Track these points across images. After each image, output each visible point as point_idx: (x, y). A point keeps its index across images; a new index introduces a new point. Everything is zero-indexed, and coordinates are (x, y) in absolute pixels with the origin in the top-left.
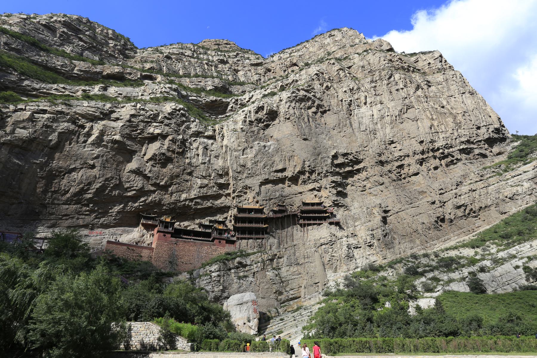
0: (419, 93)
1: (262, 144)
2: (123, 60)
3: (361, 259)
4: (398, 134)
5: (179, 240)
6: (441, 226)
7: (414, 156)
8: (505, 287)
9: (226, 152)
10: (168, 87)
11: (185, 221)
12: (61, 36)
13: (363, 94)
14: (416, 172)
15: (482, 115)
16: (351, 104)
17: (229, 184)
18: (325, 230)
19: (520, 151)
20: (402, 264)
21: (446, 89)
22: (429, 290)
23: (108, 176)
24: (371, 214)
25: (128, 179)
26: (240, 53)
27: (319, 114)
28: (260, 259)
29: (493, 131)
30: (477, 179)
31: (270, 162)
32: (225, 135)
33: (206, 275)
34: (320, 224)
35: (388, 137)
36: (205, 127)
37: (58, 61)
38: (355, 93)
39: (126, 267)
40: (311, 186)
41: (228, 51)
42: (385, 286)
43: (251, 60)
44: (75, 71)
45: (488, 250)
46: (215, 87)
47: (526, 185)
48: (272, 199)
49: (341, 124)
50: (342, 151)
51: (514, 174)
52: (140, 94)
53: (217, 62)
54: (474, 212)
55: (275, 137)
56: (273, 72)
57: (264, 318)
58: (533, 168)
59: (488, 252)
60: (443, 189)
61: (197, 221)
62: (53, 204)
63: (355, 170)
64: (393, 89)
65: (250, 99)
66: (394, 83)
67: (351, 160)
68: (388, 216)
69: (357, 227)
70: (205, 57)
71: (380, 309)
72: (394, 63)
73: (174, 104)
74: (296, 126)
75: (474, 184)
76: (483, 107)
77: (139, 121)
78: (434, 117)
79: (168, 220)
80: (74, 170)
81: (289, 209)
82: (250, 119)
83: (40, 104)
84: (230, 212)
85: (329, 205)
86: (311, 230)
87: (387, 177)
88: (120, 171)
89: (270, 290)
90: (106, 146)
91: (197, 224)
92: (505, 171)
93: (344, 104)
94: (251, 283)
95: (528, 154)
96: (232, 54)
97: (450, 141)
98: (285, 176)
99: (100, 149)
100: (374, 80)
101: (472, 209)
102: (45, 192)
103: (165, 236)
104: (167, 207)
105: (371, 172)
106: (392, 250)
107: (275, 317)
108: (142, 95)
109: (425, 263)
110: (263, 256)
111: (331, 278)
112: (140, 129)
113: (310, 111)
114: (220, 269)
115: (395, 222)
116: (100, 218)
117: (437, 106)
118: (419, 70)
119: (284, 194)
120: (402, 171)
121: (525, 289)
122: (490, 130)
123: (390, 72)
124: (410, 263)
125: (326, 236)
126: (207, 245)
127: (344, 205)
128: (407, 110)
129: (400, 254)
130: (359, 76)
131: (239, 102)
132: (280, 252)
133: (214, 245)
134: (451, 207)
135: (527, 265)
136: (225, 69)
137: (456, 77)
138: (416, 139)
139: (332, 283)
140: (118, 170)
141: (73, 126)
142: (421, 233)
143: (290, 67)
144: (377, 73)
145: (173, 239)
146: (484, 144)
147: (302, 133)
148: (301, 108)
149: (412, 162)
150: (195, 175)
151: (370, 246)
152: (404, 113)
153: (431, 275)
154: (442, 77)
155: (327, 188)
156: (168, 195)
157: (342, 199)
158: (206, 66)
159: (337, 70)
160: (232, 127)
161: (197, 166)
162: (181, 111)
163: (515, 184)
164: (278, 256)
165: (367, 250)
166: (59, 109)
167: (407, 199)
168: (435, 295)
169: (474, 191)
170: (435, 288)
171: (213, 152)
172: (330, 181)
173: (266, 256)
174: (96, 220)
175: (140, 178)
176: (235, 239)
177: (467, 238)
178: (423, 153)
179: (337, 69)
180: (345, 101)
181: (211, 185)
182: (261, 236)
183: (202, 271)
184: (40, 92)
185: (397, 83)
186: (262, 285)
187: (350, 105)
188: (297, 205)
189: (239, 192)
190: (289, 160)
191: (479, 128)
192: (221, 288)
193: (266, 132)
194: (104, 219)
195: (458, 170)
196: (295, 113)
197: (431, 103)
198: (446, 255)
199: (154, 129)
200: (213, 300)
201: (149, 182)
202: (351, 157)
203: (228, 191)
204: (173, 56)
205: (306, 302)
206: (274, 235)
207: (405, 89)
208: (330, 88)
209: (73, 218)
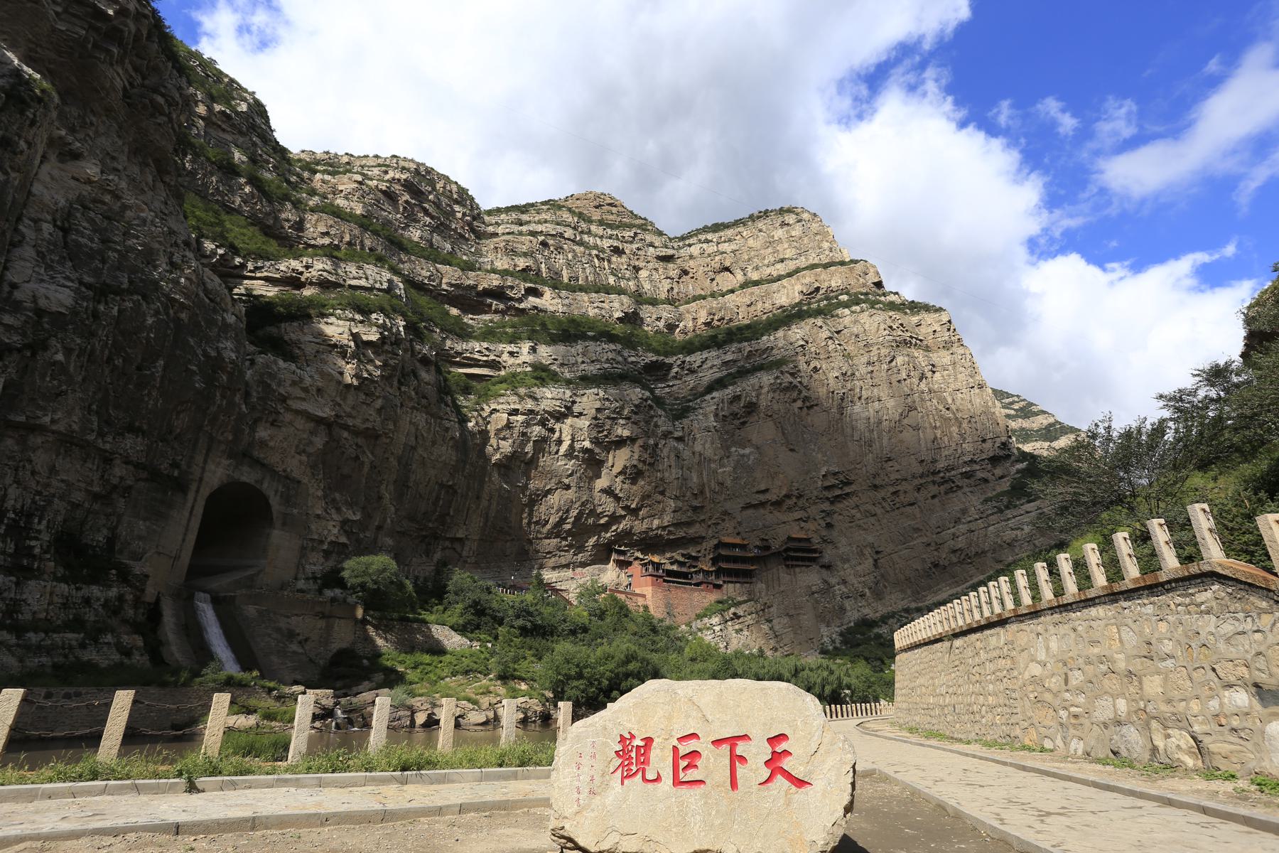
1: (742, 452)
12: (405, 208)
20: (895, 620)
24: (861, 554)
33: (708, 629)
40: (797, 515)
44: (444, 286)
47: (1027, 529)
52: (580, 360)
53: (608, 251)
61: (668, 555)
62: (537, 538)
64: (894, 380)
65: (703, 362)
66: (895, 370)
78: (938, 424)
80: (549, 492)
84: (704, 544)
92: (1007, 507)
99: (573, 461)
117: (941, 407)
118: (921, 340)
122: (997, 445)
126: (696, 590)
130: (850, 348)
133: (702, 590)
140: (591, 489)
158: (596, 260)
162: (649, 402)
167: (901, 538)
175: (611, 499)
178: (921, 477)
182: (749, 580)
184: (464, 358)
187: (842, 399)
191: (984, 441)
202: (842, 477)
204: (551, 242)
209: (555, 555)
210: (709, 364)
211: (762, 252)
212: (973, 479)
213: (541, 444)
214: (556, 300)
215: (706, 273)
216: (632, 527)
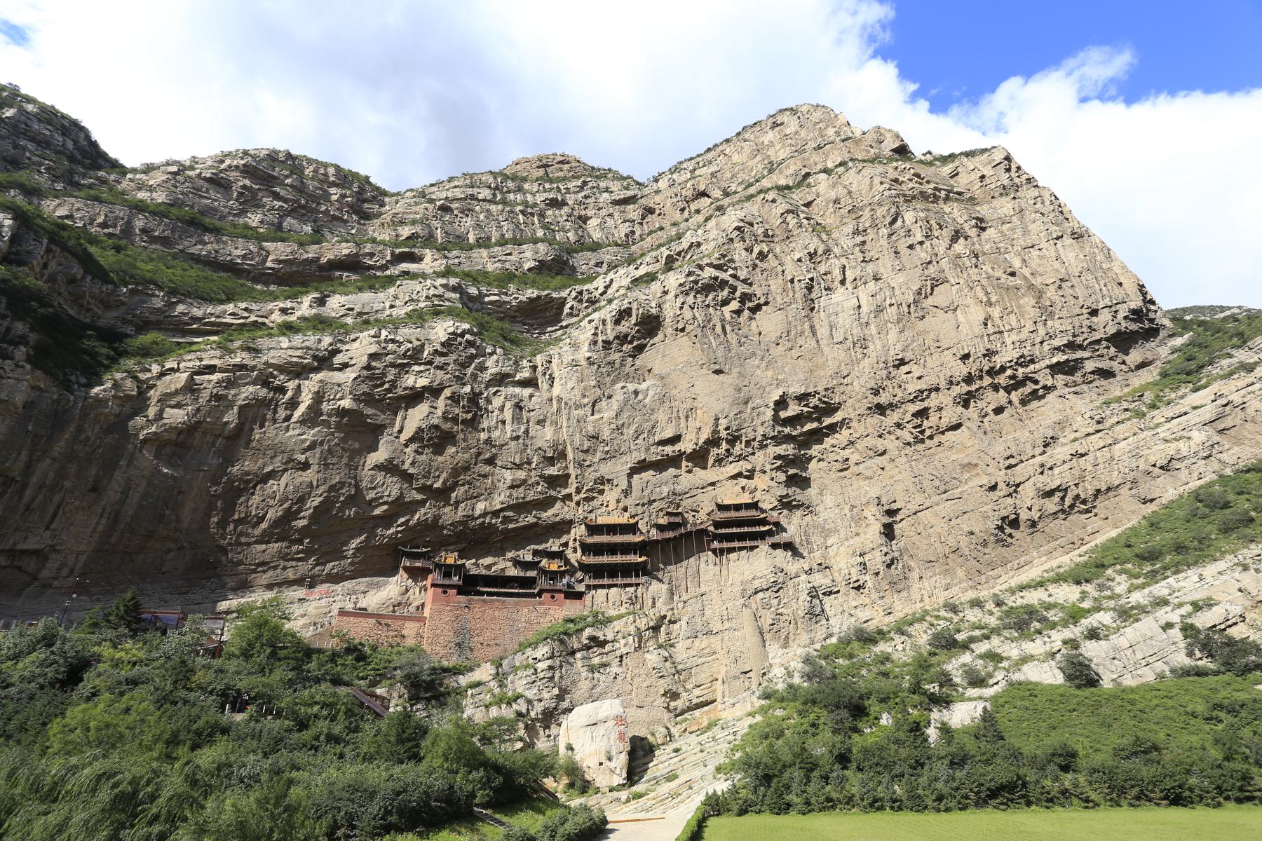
0: (960, 247)
1: (631, 387)
2: (359, 223)
3: (839, 616)
4: (915, 344)
5: (473, 600)
6: (1011, 536)
7: (949, 389)
8: (1139, 672)
9: (558, 410)
10: (441, 285)
11: (483, 556)
12: (240, 194)
13: (837, 262)
14: (955, 423)
15: (1102, 283)
16: (813, 287)
17: (568, 476)
18: (764, 560)
19: (1188, 360)
20: (926, 624)
21: (1019, 232)
22: (977, 681)
23: (334, 482)
24: (859, 519)
25: (372, 482)
26: (589, 179)
27: (746, 313)
28: (632, 629)
29: (1126, 318)
30: (1091, 430)
31: (648, 425)
32: (556, 375)
34: (752, 548)
35: (892, 353)
36: (516, 363)
37: (236, 248)
38: (820, 262)
39: (375, 660)
40: (732, 469)
41: (564, 179)
42: (885, 675)
43: (612, 192)
44: (269, 264)
45: (1109, 588)
46: (539, 261)
47: (1198, 436)
48: (654, 501)
49: (793, 332)
50: (796, 389)
51: (1171, 415)
52: (388, 305)
53: (543, 206)
54: (1084, 502)
55: (655, 371)
56: (659, 215)
57: (643, 749)
58: (1213, 398)
59: (1109, 593)
60: (1013, 457)
61: (510, 555)
62: (239, 544)
63: (826, 427)
64: (902, 246)
65: (607, 287)
67: (815, 407)
68: (895, 522)
69: (830, 550)
70: (519, 197)
71: (869, 730)
72: (904, 187)
73: (452, 322)
74: (698, 344)
75: (1083, 441)
76: (1104, 266)
77: (386, 366)
78: (994, 299)
79: (450, 561)
80: (272, 475)
81: (691, 520)
82: (604, 338)
83: (204, 355)
84: (573, 531)
85: (771, 507)
86: (734, 561)
87: (892, 437)
88: (357, 468)
89: (652, 689)
90: (326, 424)
91: (509, 560)
92: (1153, 406)
93: (797, 289)
94: (615, 678)
95: (1202, 367)
96: (574, 184)
97: (1029, 348)
98: (680, 451)
99: (316, 429)
100: (861, 229)
101: (1078, 496)
102: (223, 524)
103: (445, 592)
104: (450, 530)
105: (858, 428)
106: (904, 594)
107: (663, 744)
108: (392, 307)
109: (973, 619)
110: (638, 621)
111: (777, 661)
112: (388, 382)
113: (727, 310)
114: (553, 653)
115: (912, 534)
116: (324, 564)
117: (999, 273)
118: (960, 194)
119: (679, 489)
120: (925, 421)
121: (1182, 676)
122: (1121, 315)
123: (893, 210)
124: (941, 622)
125: (766, 572)
126: (527, 605)
127: (803, 504)
128: (932, 289)
129: (922, 600)
130: (829, 220)
131: (585, 297)
132: (672, 609)
133: (541, 604)
134: (1031, 495)
135: (1189, 621)
136: (560, 219)
137: (1043, 203)
138: (954, 350)
139: (778, 672)
140: (353, 467)
141: (265, 390)
142: (968, 553)
143: (693, 200)
144: (867, 213)
145: (462, 598)
146: (1108, 348)
147: (710, 360)
148: (708, 306)
149: (945, 402)
150: (499, 463)
151: (858, 588)
152: (926, 297)
153: (982, 647)
154: (1010, 205)
155: (765, 472)
156: (451, 508)
157: (798, 491)
158: (521, 217)
159: (782, 214)
160: (568, 358)
161: (503, 445)
162: (467, 336)
163: (1174, 436)
164: (668, 618)
165: (851, 598)
166: (237, 360)
167: (937, 483)
168: (988, 692)
169: (1082, 455)
170: (991, 676)
171: (532, 413)
172: (772, 456)
173: (644, 620)
174: (317, 568)
175: (395, 479)
176: (581, 588)
177: (1066, 560)
178: (969, 379)
179: (781, 211)
180: (799, 281)
181: (533, 480)
182: (633, 580)
183: (519, 659)
184: (206, 324)
185: (909, 231)
186: (637, 681)
187: (810, 288)
188: (707, 510)
189: (587, 490)
190: (687, 417)
191: (1094, 313)
192: (556, 691)
193: (638, 362)
194: (332, 564)
195: (1048, 411)
196: (694, 318)
197: (987, 268)
198: (1020, 602)
199: (416, 379)
200: (540, 716)
201: (411, 485)
202: (814, 401)
203: (568, 491)
204: (454, 205)
205: (726, 712)
206: (660, 574)
207: (928, 244)
208: (767, 256)
209: (275, 568)
210: (615, 286)
211: (750, 164)
212: (1079, 374)
213: (255, 413)
214: (439, 261)
215: (674, 204)
216: (437, 518)
